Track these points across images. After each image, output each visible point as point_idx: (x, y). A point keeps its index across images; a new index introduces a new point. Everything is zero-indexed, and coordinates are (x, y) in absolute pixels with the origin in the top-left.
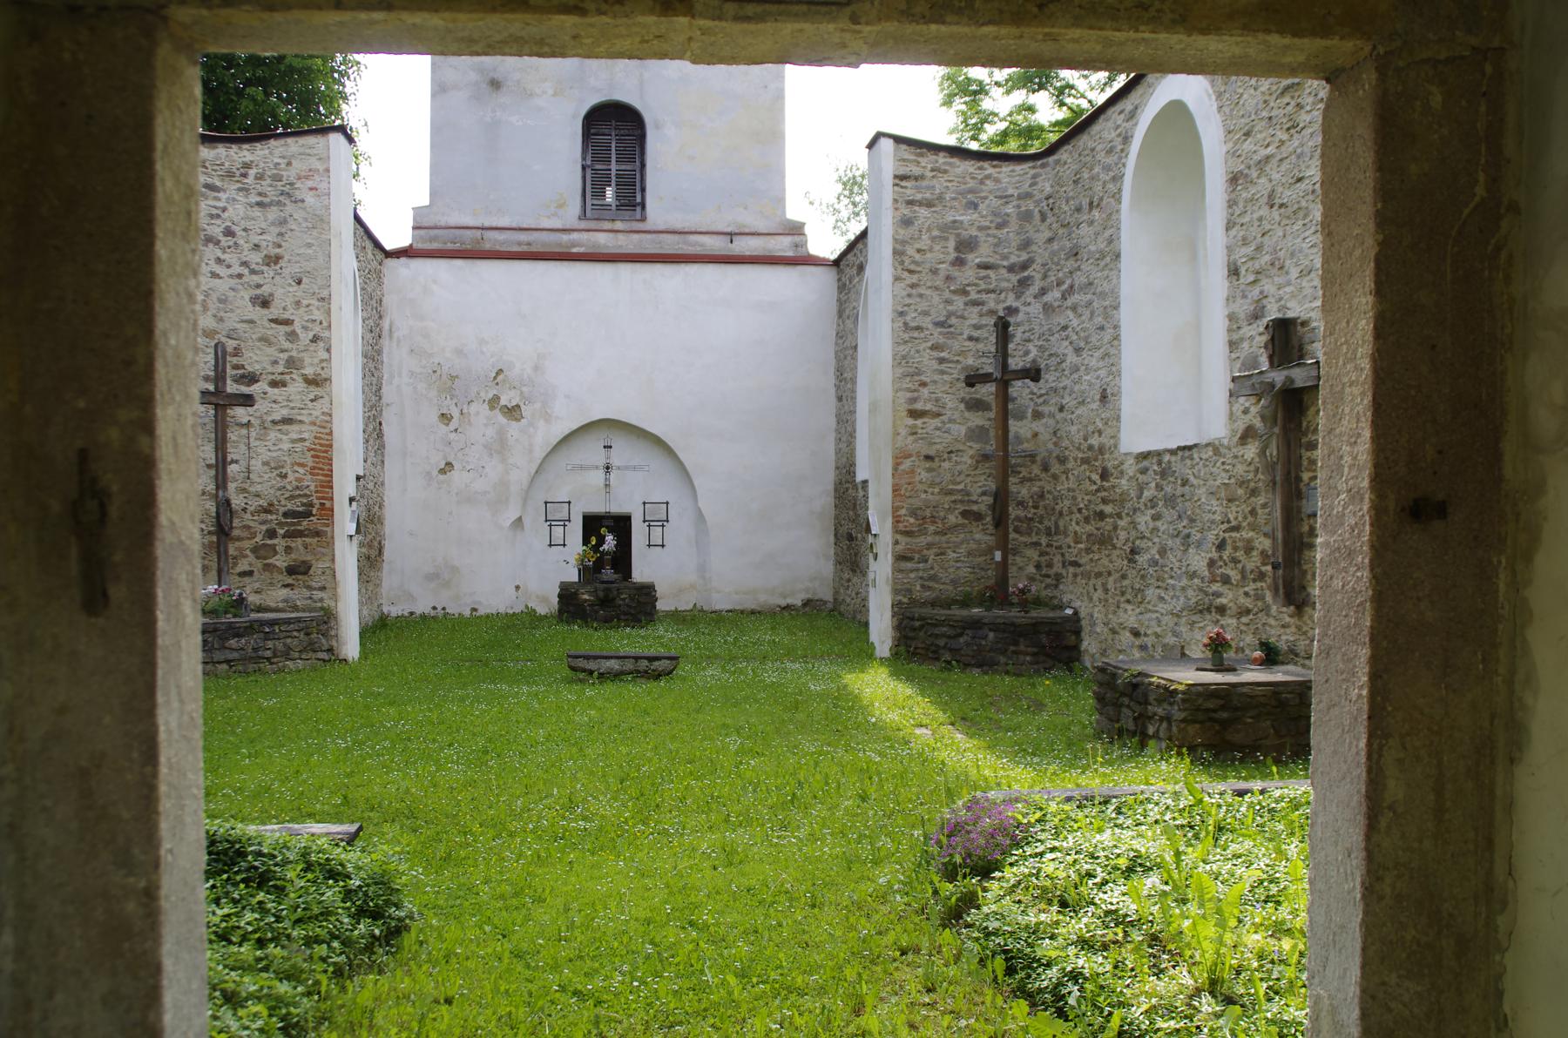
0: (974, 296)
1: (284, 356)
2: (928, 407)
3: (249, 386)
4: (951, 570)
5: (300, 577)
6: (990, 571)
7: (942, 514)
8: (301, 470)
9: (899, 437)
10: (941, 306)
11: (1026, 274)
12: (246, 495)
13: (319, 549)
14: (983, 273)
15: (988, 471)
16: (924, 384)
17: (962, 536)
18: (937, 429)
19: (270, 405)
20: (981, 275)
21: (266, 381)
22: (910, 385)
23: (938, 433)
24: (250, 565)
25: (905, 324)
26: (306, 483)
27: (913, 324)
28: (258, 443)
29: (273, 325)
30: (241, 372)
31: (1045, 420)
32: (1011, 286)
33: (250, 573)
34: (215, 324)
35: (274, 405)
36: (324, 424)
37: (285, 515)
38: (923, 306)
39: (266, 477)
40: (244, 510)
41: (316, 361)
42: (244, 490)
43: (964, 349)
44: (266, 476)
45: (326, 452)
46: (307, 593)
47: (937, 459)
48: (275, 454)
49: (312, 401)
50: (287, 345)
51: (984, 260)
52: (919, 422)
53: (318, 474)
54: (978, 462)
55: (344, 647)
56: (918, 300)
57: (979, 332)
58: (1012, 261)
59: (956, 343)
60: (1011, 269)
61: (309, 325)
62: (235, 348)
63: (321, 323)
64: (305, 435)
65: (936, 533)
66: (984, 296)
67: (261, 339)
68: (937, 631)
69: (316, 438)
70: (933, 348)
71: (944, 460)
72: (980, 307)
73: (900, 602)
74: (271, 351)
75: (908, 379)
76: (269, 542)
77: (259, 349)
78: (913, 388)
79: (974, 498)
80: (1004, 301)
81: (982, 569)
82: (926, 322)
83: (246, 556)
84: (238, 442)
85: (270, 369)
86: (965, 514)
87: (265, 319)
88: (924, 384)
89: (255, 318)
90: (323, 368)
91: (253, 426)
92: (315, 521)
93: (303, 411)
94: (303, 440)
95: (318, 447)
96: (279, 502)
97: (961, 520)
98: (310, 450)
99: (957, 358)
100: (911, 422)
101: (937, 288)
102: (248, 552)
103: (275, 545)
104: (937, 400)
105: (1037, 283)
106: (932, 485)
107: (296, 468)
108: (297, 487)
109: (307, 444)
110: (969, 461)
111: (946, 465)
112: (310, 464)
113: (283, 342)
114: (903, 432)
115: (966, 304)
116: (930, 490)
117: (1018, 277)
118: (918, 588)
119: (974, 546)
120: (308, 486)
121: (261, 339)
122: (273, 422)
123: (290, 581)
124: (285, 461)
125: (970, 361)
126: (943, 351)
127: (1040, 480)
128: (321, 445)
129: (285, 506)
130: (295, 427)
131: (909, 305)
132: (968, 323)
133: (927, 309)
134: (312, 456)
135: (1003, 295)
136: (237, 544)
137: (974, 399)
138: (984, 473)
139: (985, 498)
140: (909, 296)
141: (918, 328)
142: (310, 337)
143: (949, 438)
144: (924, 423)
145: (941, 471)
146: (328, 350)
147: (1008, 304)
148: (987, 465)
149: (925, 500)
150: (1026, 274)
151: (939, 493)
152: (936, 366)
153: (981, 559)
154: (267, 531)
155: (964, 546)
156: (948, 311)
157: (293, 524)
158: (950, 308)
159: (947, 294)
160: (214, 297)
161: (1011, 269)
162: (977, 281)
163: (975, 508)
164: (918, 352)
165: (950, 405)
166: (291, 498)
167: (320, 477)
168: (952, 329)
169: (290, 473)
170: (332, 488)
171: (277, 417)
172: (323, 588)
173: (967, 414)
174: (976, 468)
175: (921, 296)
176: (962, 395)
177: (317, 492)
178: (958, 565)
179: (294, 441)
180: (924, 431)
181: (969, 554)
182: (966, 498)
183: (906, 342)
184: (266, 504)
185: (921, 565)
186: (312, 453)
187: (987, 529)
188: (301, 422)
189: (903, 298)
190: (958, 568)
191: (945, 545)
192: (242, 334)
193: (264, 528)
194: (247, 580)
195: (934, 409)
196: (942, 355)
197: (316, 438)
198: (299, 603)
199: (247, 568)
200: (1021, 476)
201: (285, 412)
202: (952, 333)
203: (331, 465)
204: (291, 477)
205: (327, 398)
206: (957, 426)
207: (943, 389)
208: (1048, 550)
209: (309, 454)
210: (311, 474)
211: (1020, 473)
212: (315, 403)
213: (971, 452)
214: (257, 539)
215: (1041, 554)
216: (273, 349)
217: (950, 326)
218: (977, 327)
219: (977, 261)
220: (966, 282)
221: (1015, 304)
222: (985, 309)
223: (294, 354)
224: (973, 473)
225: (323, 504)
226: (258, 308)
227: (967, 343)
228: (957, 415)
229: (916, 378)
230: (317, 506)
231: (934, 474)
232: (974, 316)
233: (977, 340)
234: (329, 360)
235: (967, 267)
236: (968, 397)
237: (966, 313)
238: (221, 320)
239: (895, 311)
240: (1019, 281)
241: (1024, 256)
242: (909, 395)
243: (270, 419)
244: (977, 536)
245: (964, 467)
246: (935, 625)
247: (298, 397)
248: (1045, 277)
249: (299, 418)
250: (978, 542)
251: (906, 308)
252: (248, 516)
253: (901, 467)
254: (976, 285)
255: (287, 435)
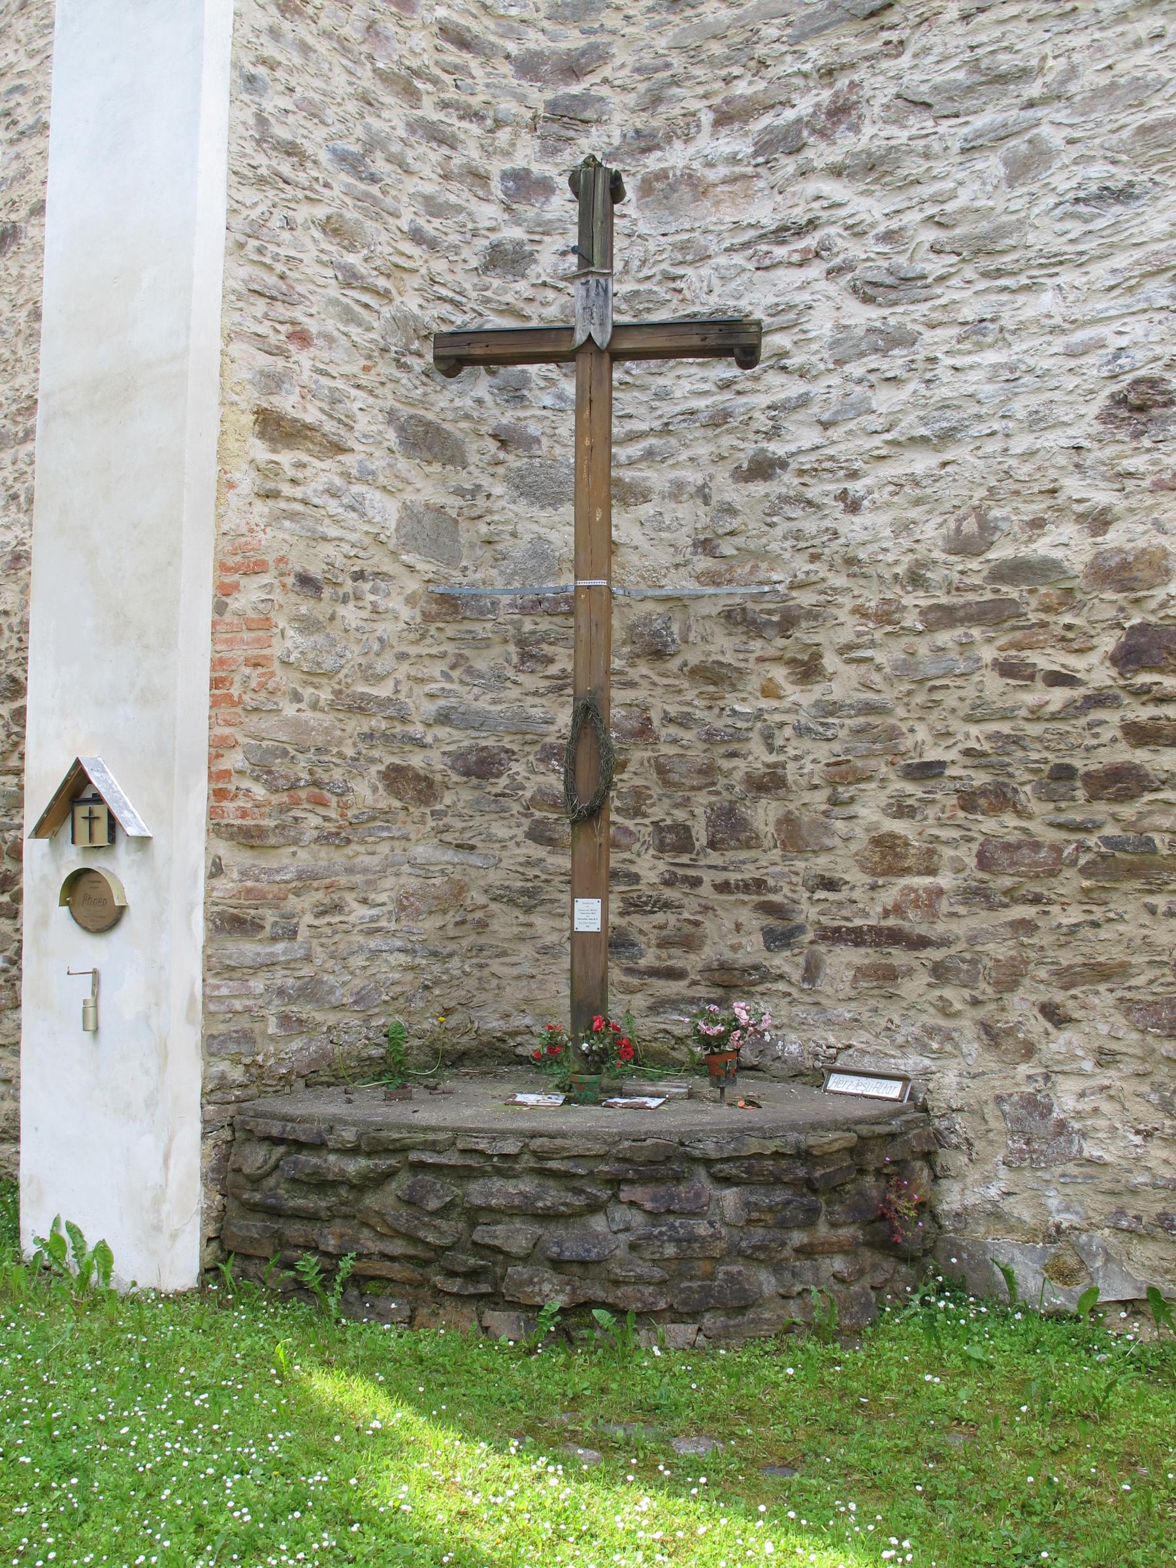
0: (429, 111)
2: (311, 415)
4: (358, 961)
6: (455, 962)
7: (337, 774)
9: (231, 495)
10: (352, 107)
11: (576, 89)
14: (453, 55)
15: (450, 648)
16: (301, 337)
17: (384, 848)
18: (333, 493)
20: (450, 59)
22: (264, 329)
23: (333, 506)
25: (261, 120)
27: (281, 132)
31: (646, 510)
32: (529, 114)
38: (307, 86)
43: (401, 261)
47: (327, 592)
51: (455, 17)
52: (286, 458)
54: (427, 617)
56: (297, 60)
57: (436, 222)
58: (532, 46)
59: (384, 237)
60: (528, 67)
65: (324, 839)
66: (454, 120)
68: (477, 1192)
70: (333, 228)
71: (345, 600)
72: (444, 150)
73: (223, 1084)
75: (261, 305)
78: (273, 339)
79: (417, 730)
80: (507, 154)
81: (435, 954)
82: (314, 140)
86: (395, 777)
88: (301, 337)
97: (385, 801)
99: (382, 283)
100: (260, 451)
101: (343, 46)
104: (335, 399)
105: (618, 118)
106: (314, 675)
110: (406, 613)
111: (350, 614)
114: (247, 482)
115: (411, 127)
116: (307, 692)
117: (549, 95)
118: (272, 1029)
119: (413, 883)
125: (412, 303)
126: (352, 248)
127: (631, 685)
131: (272, 64)
132: (412, 185)
133: (317, 97)
135: (504, 135)
137: (421, 421)
138: (443, 656)
139: (443, 732)
140: (275, 33)
141: (291, 150)
143: (358, 531)
144: (301, 465)
145: (335, 632)
147: (519, 162)
148: (451, 630)
149: (299, 727)
150: (576, 89)
151: (332, 705)
152: (334, 291)
153: (430, 924)
155: (389, 882)
156: (368, 128)
158: (376, 124)
159: (366, 79)
161: (528, 67)
162: (437, 71)
163: (416, 760)
164: (289, 224)
165: (362, 423)
168: (375, 190)
173: (403, 464)
174: (423, 636)
175: (305, 49)
176: (390, 403)
178: (374, 943)
180: (298, 492)
181: (401, 906)
182: (399, 729)
183: (262, 181)
185: (280, 947)
187: (447, 829)
189: (257, 32)
190: (375, 954)
191: (343, 880)
195: (329, 426)
196: (351, 259)
200: (553, 670)
202: (375, 201)
206: (378, 495)
207: (347, 369)
208: (669, 894)
211: (551, 661)
213: (413, 585)
215: (633, 906)
217: (373, 179)
218: (434, 207)
219: (441, 12)
220: (415, 63)
221: (539, 169)
222: (457, 161)
224: (413, 650)
227: (408, 247)
228: (379, 463)
229: (280, 310)
231: (319, 639)
232: (427, 172)
233: (432, 245)
235: (417, 23)
236: (405, 411)
237: (410, 155)
239: (236, 65)
240: (552, 105)
241: (572, 40)
242: (263, 360)
244: (421, 851)
245: (385, 628)
246: (465, 1174)
248: (655, 100)
250: (423, 869)
251: (261, 71)
253: (237, 603)
254: (435, 81)
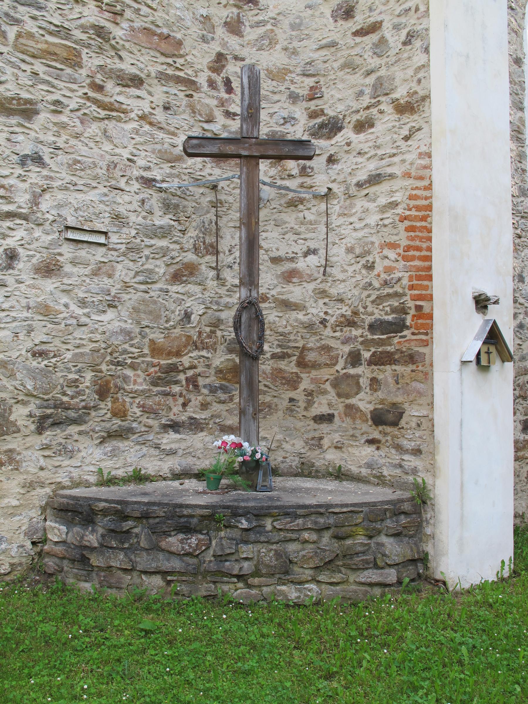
1: (371, 80)
3: (329, 138)
5: (388, 429)
8: (392, 254)
12: (326, 300)
13: (414, 384)
19: (355, 160)
21: (351, 126)
24: (330, 405)
26: (398, 275)
28: (341, 221)
29: (358, 39)
30: (319, 120)
33: (328, 418)
34: (286, 61)
35: (360, 159)
36: (421, 173)
37: (372, 328)
39: (351, 269)
40: (323, 322)
41: (410, 72)
42: (323, 293)
44: (351, 269)
45: (424, 219)
46: (395, 457)
48: (360, 234)
49: (406, 138)
50: (374, 62)
53: (413, 258)
55: (443, 559)
61: (403, 20)
62: (312, 88)
63: (417, 9)
64: (398, 197)
67: (343, 67)
69: (411, 198)
74: (357, 79)
76: (352, 371)
77: (343, 81)
83: (325, 392)
84: (316, 222)
85: (355, 106)
87: (349, 33)
89: (335, 36)
90: (419, 81)
91: (335, 196)
92: (410, 337)
93: (396, 159)
94: (394, 205)
95: (414, 213)
96: (365, 308)
98: (403, 219)
102: (328, 386)
103: (359, 376)
107: (386, 252)
108: (386, 283)
109: (399, 210)
112: (404, 243)
113: (369, 60)
120: (399, 279)
121: (343, 67)
122: (359, 185)
123: (376, 435)
124: (373, 243)
128: (418, 208)
129: (372, 314)
130: (384, 187)
134: (408, 229)
136: (314, 373)
142: (403, 37)
146: (427, 50)
154: (350, 354)
157: (381, 342)
160: (286, 23)
166: (380, 299)
167: (417, 263)
169: (378, 260)
170: (430, 278)
171: (362, 176)
172: (417, 452)
177: (412, 288)
179: (384, 209)
184: (349, 313)
186: (407, 223)
188: (392, 176)
192: (322, 66)
193: (347, 349)
194: (325, 427)
197: (411, 198)
198: (385, 473)
199: (324, 410)
201: (372, 166)
203: (430, 239)
204: (379, 268)
205: (425, 130)
209: (402, 226)
210: (406, 259)
212: (409, 143)
214: (338, 367)
216: (357, 75)
223: (382, 72)
225: (419, 308)
226: (341, 22)
230: (413, 312)
234: (425, 66)
238: (295, 53)
243: (354, 181)
247: (388, 138)
249: (389, 170)
252: (328, 332)
255: (374, 201)
